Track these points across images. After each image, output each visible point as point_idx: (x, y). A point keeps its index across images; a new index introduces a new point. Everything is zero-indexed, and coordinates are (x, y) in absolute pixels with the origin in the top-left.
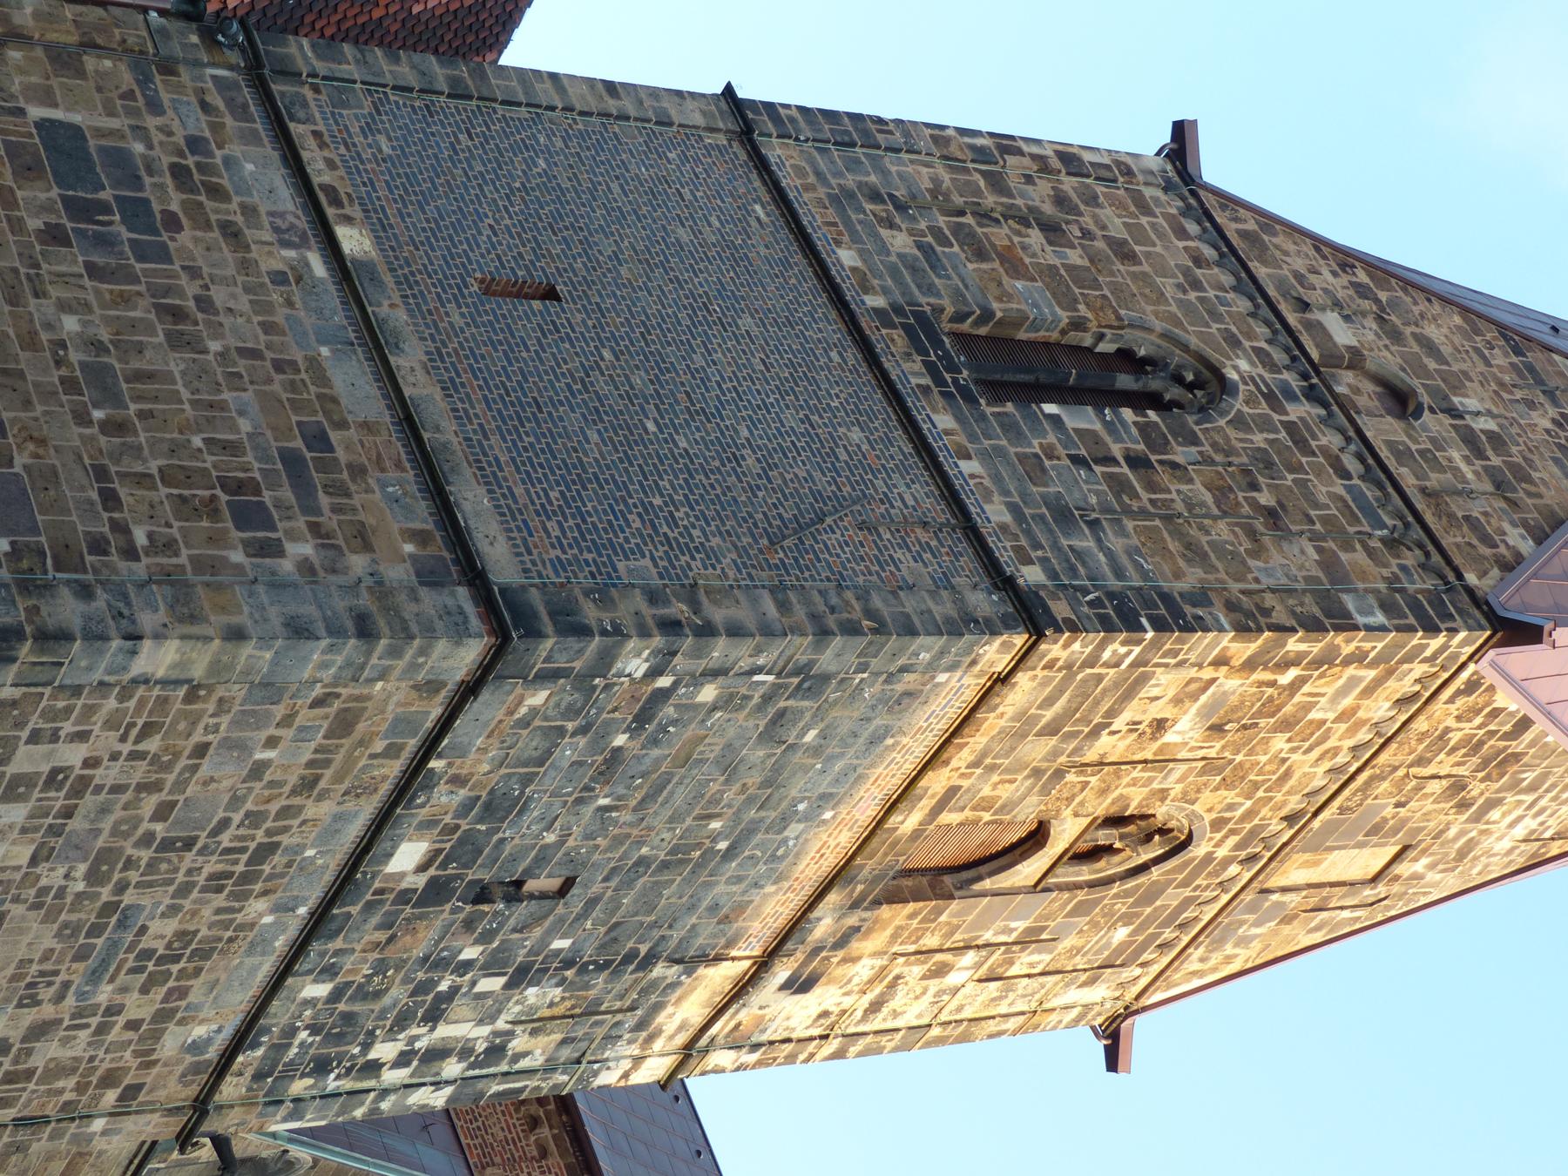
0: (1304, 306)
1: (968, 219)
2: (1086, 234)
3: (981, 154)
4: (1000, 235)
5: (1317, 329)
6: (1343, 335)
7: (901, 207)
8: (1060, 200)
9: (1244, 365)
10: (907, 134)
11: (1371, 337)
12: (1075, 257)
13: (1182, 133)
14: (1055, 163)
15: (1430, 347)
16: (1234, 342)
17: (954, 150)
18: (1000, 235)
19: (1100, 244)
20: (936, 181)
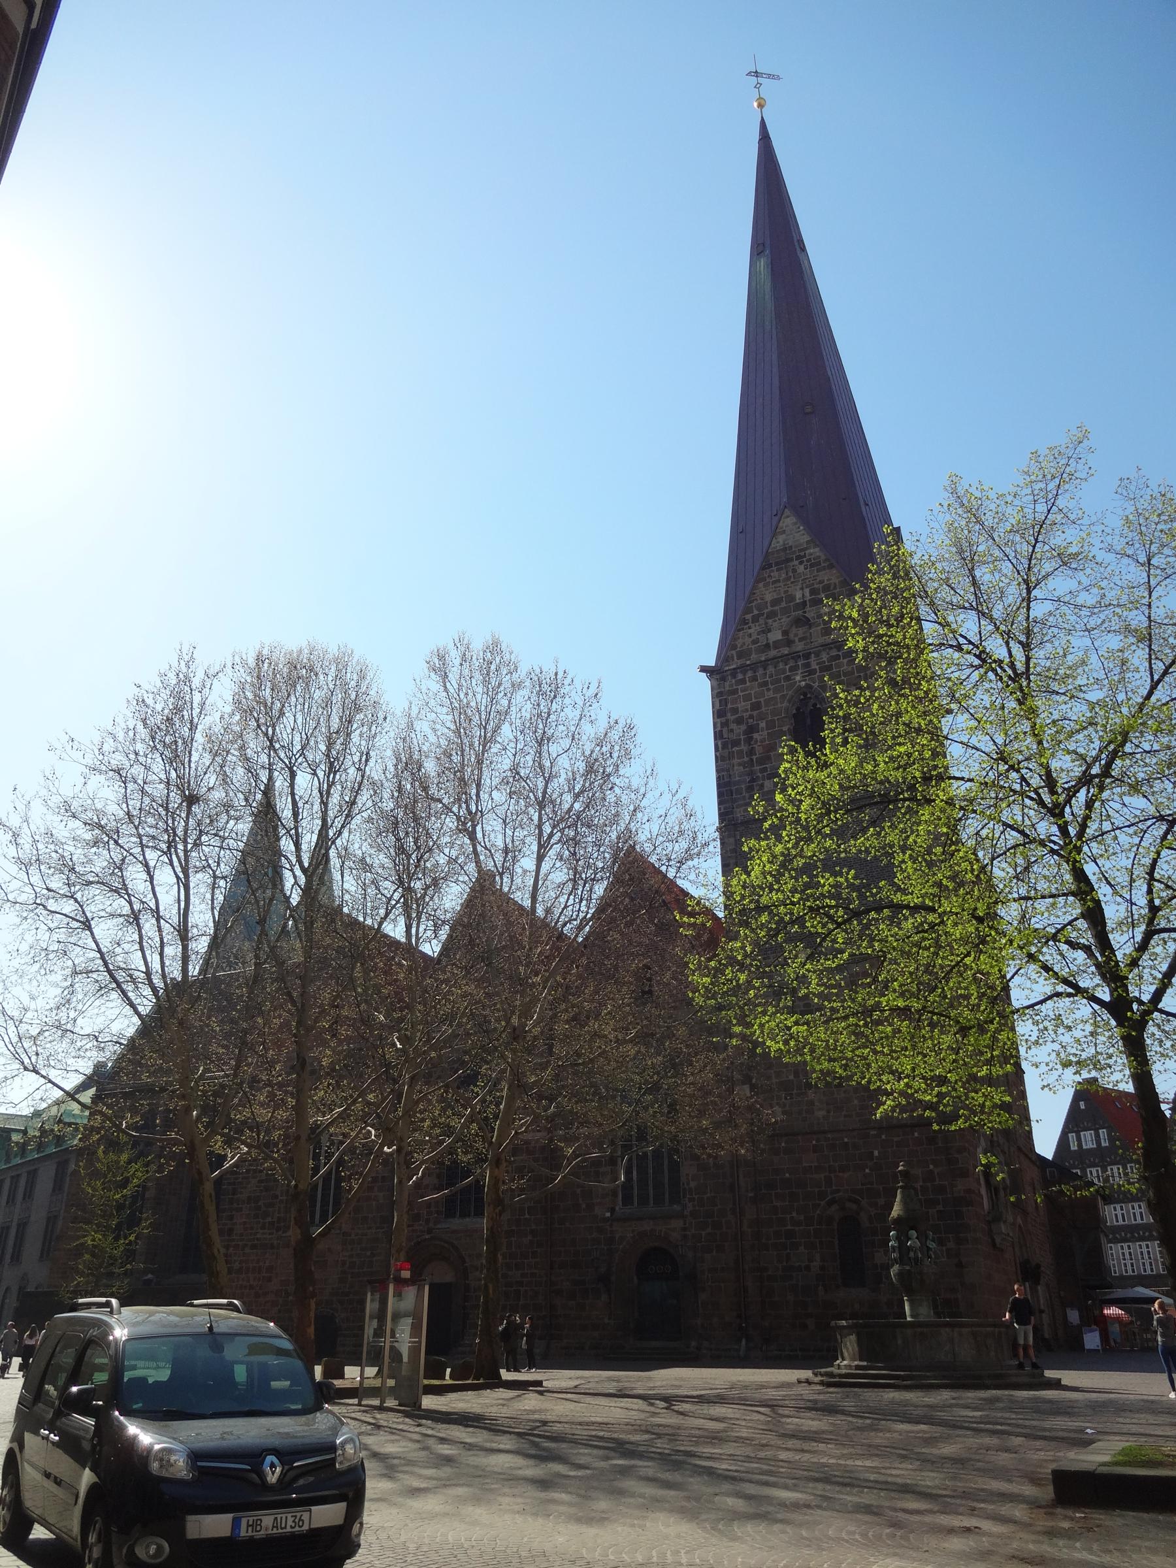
0: (767, 646)
1: (754, 758)
2: (751, 717)
3: (725, 746)
4: (759, 750)
5: (777, 645)
6: (776, 636)
7: (753, 780)
8: (739, 721)
9: (798, 678)
10: (723, 770)
11: (775, 624)
12: (763, 725)
13: (704, 669)
14: (723, 719)
15: (775, 602)
16: (788, 678)
17: (726, 755)
18: (759, 750)
19: (755, 713)
20: (739, 764)
